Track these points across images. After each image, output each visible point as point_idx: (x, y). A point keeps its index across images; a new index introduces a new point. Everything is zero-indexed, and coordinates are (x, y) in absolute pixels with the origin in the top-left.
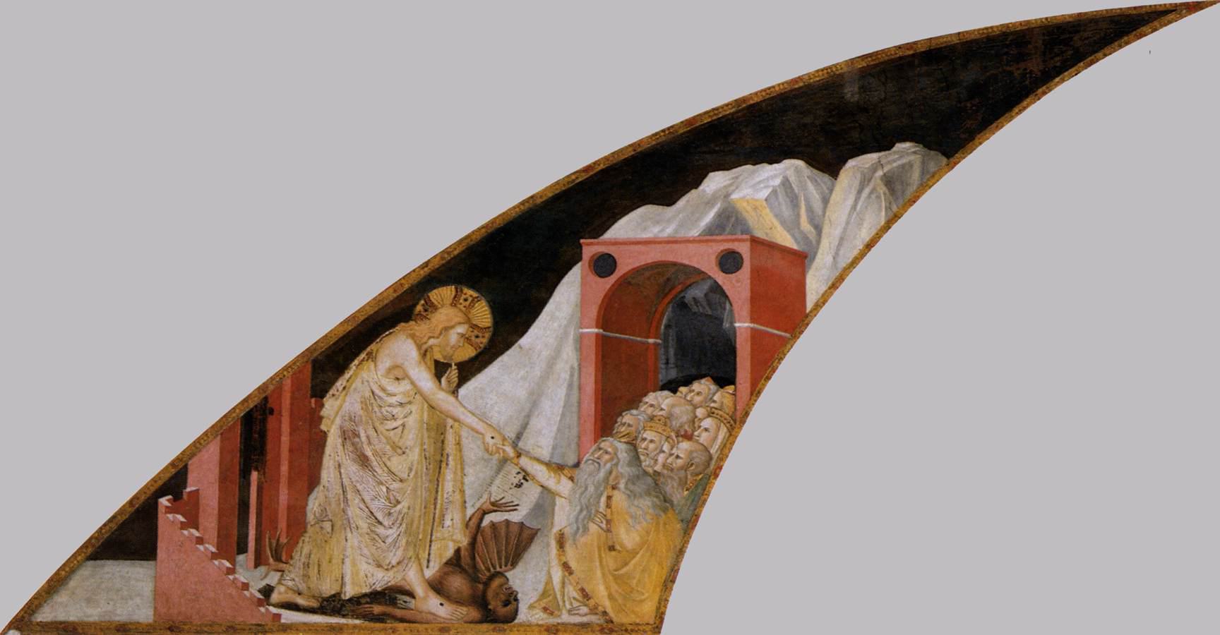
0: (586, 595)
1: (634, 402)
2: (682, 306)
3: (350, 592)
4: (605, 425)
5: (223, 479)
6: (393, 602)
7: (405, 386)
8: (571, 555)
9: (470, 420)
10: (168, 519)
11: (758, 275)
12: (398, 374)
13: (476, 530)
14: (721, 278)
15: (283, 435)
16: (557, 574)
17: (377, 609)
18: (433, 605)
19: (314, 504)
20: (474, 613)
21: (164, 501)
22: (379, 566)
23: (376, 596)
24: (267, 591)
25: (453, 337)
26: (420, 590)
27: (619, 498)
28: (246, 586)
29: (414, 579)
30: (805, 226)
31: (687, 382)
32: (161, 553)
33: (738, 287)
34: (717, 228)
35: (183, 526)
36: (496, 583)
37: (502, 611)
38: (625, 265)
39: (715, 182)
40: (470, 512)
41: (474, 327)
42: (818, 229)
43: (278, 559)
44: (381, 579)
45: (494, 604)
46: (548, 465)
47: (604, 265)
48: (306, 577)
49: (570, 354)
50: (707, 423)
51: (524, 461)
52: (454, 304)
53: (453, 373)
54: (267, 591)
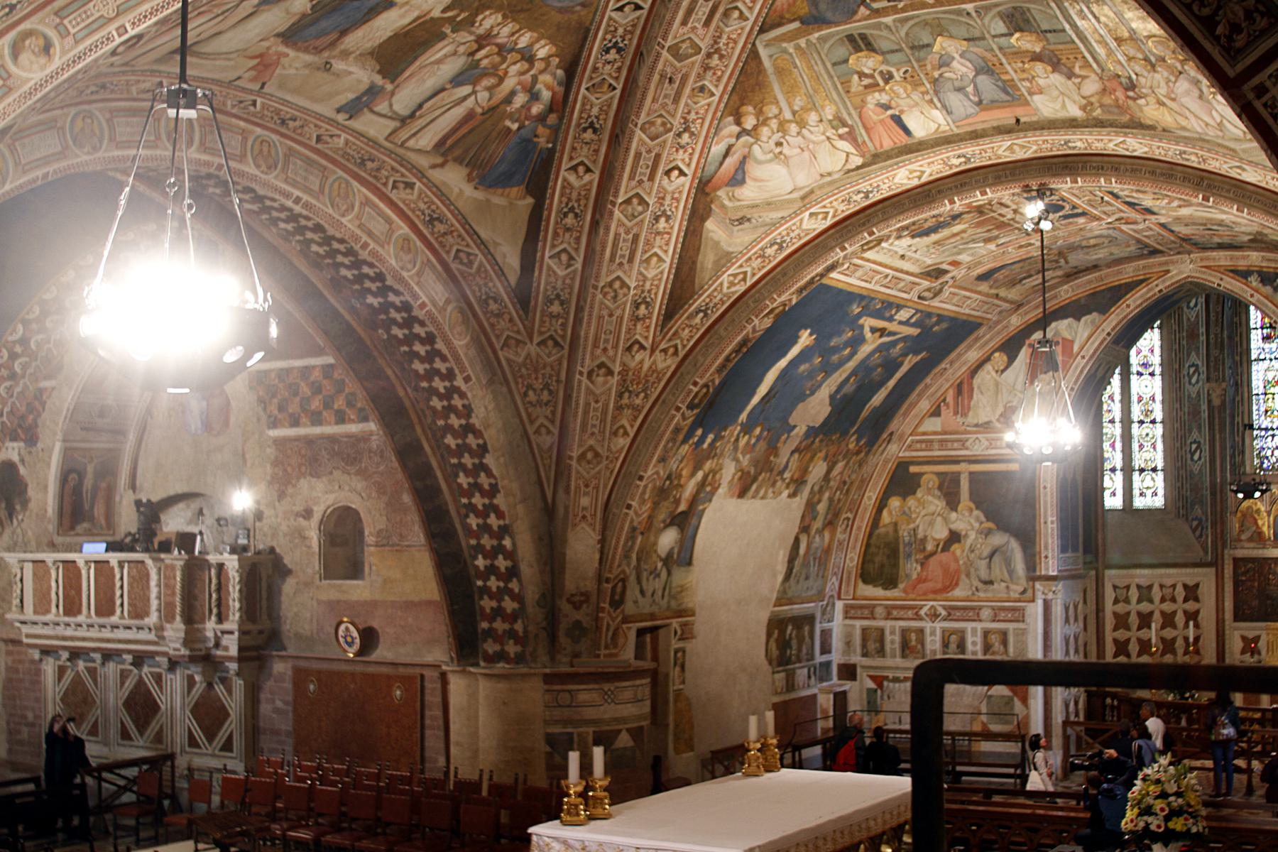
10: (943, 408)
12: (988, 373)
15: (965, 387)
44: (986, 420)
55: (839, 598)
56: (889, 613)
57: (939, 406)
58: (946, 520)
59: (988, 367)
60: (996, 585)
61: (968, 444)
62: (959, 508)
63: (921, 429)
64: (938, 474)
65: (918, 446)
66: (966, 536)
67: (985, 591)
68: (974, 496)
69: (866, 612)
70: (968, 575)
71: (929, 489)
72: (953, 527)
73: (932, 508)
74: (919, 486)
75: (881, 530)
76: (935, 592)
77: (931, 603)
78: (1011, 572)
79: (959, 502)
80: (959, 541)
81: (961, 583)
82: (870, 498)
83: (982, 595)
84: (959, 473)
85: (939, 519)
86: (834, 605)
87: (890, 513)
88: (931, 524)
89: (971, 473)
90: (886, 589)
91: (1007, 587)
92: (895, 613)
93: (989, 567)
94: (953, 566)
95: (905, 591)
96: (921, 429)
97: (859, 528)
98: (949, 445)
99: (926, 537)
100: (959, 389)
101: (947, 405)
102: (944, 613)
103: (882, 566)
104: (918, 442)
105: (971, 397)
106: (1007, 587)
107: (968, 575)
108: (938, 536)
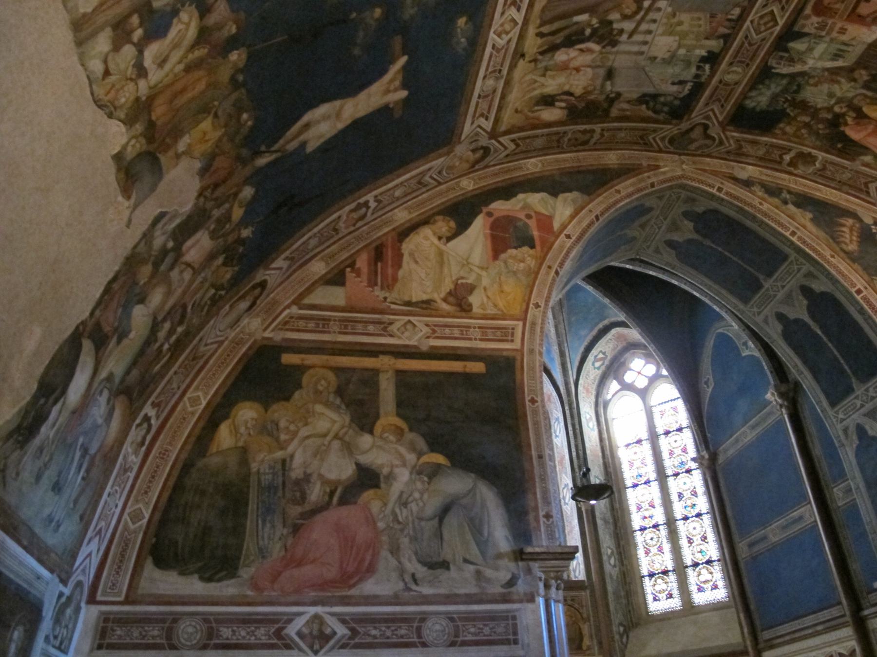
0: (495, 306)
1: (504, 251)
2: (516, 227)
3: (414, 300)
4: (496, 257)
5: (369, 265)
6: (430, 304)
8: (490, 294)
9: (451, 253)
10: (349, 274)
11: (538, 221)
12: (426, 238)
13: (456, 285)
14: (527, 220)
15: (389, 253)
17: (424, 306)
18: (445, 306)
19: (401, 273)
20: (458, 309)
21: (348, 270)
22: (424, 293)
23: (423, 302)
24: (385, 298)
25: (444, 230)
26: (439, 301)
27: (503, 278)
28: (378, 296)
29: (438, 297)
30: (551, 210)
31: (520, 247)
32: (348, 284)
33: (532, 223)
34: (523, 208)
35: (355, 277)
36: (464, 300)
37: (468, 308)
38: (497, 215)
39: (521, 196)
40: (454, 279)
41: (450, 227)
42: (554, 210)
43: (389, 289)
44: (425, 297)
45: (465, 307)
47: (490, 214)
48: (399, 295)
49: (481, 237)
50: (529, 258)
51: (470, 266)
52: (443, 221)
53: (444, 240)
54: (385, 298)
55: (92, 600)
56: (211, 633)
57: (342, 273)
58: (349, 448)
59: (426, 231)
60: (453, 573)
61: (394, 328)
62: (378, 428)
63: (307, 301)
64: (338, 370)
65: (302, 324)
66: (391, 477)
67: (431, 583)
68: (402, 408)
69: (154, 631)
70: (395, 550)
71: (317, 392)
72: (364, 459)
73: (322, 425)
74: (299, 386)
75: (213, 461)
76: (324, 585)
77: (312, 610)
78: (482, 543)
79: (377, 417)
80: (377, 486)
81: (381, 566)
82: (195, 401)
83: (426, 590)
84: (376, 372)
85: (336, 444)
86: (78, 610)
87: (235, 431)
88: (320, 453)
89: (399, 373)
90: (209, 580)
91: (478, 573)
92: (226, 632)
93: (439, 535)
94: (363, 534)
95: (255, 586)
96: (307, 301)
97: (164, 454)
98: (360, 327)
99: (307, 478)
100: (378, 254)
101: (358, 273)
102: (341, 631)
103: (206, 530)
104: (301, 318)
105: (398, 265)
106: (478, 573)
107: (395, 550)
108: (332, 476)
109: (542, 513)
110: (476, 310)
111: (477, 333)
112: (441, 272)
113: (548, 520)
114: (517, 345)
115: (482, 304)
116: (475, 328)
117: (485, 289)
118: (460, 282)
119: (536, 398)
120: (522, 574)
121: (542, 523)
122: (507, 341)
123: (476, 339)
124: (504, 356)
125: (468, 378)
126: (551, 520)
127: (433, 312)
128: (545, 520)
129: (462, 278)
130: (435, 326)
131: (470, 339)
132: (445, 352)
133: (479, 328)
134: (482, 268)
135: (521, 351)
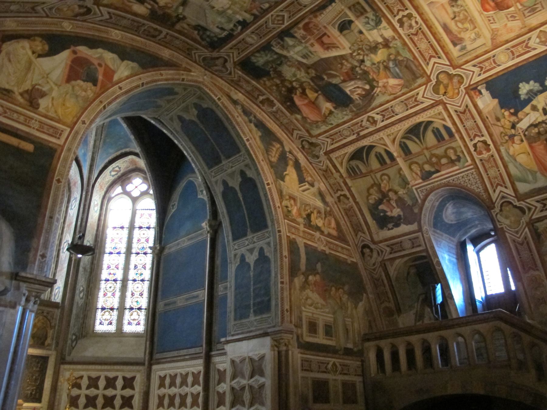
0: (56, 112)
1: (75, 80)
7: (24, 51)
11: (105, 70)
13: (33, 87)
16: (50, 105)
18: (19, 98)
20: (29, 104)
26: (17, 93)
29: (15, 89)
31: (87, 81)
34: (99, 58)
36: (35, 100)
37: (37, 107)
38: (79, 55)
39: (100, 50)
40: (33, 83)
44: (7, 87)
46: (54, 83)
47: (75, 52)
49: (63, 65)
50: (90, 91)
51: (48, 79)
59: (26, 44)
109: (39, 253)
110: (41, 109)
111: (37, 125)
112: (26, 74)
113: (42, 258)
114: (61, 142)
115: (48, 107)
116: (36, 120)
117: (53, 99)
118: (37, 87)
119: (61, 180)
120: (12, 289)
121: (37, 259)
122: (56, 137)
123: (34, 128)
124: (50, 147)
125: (18, 152)
126: (44, 259)
127: (10, 99)
128: (40, 258)
129: (39, 85)
130: (8, 109)
131: (30, 127)
132: (9, 129)
133: (39, 122)
134: (56, 85)
135: (63, 147)
